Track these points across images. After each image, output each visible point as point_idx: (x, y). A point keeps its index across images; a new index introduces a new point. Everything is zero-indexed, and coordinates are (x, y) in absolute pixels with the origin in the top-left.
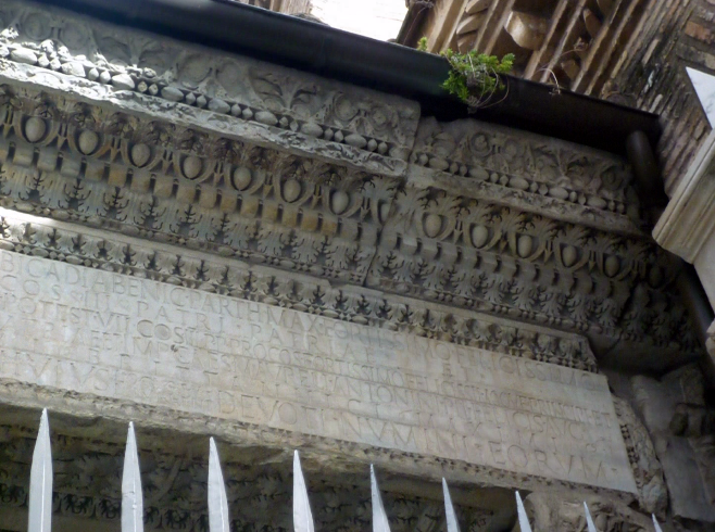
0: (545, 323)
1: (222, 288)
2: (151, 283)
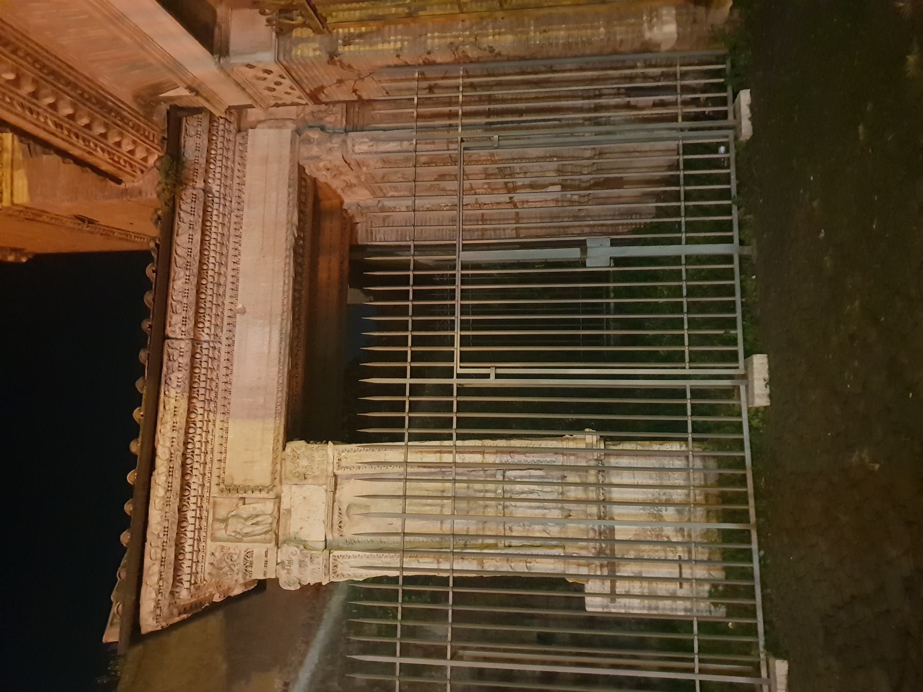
2: (241, 263)
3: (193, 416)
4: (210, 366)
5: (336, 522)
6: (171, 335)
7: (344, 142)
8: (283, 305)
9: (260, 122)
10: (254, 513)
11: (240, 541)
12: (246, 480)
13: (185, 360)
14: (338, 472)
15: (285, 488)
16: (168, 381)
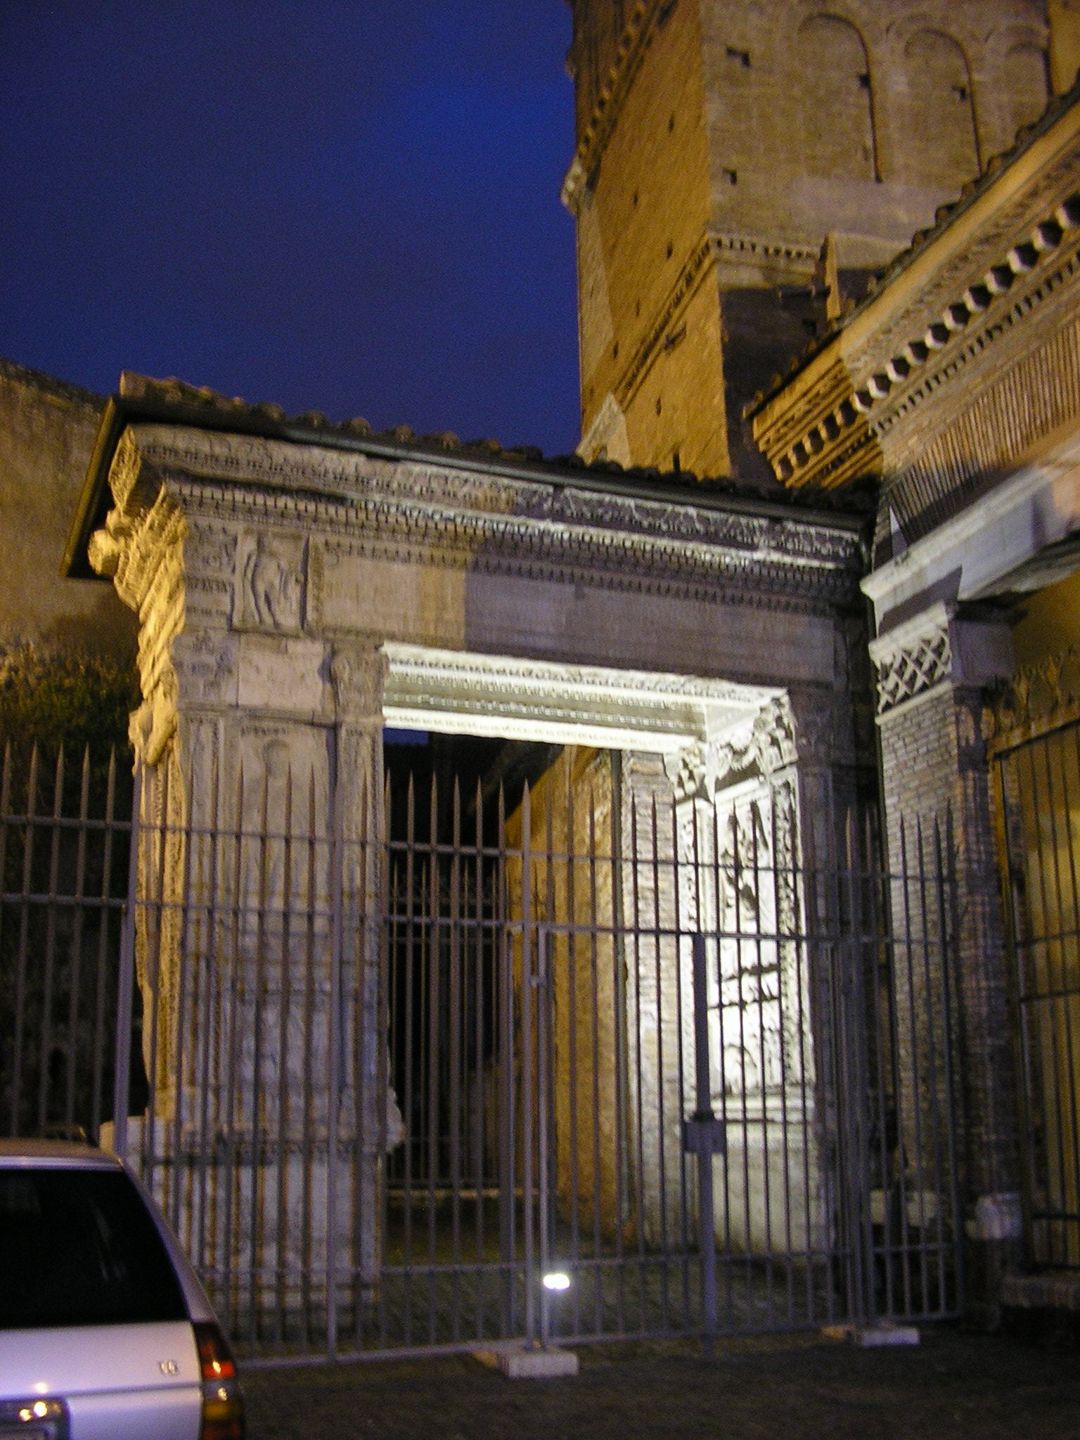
1: (677, 594)
12: (331, 586)
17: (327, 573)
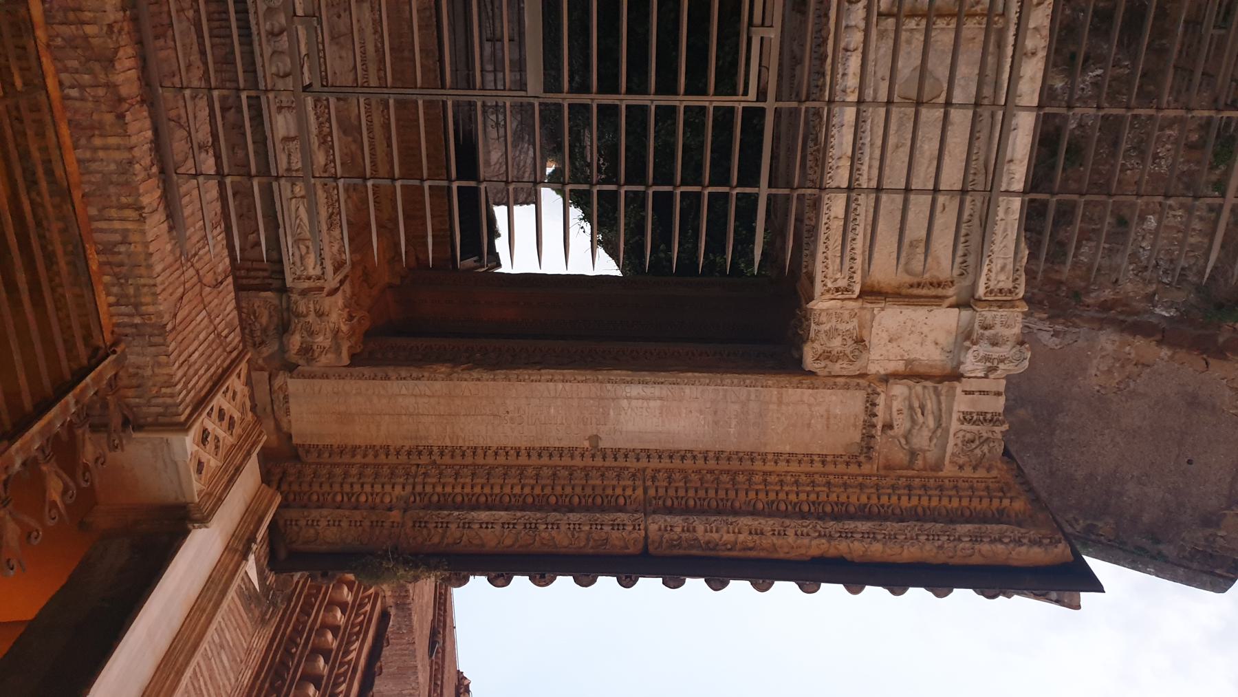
0: (325, 464)
1: (486, 450)
2: (518, 445)
3: (760, 506)
4: (682, 484)
5: (933, 292)
6: (640, 546)
7: (304, 293)
8: (586, 381)
9: (278, 427)
10: (905, 411)
11: (947, 431)
12: (855, 426)
13: (678, 521)
14: (857, 289)
15: (873, 369)
16: (711, 546)
17: (857, 438)
